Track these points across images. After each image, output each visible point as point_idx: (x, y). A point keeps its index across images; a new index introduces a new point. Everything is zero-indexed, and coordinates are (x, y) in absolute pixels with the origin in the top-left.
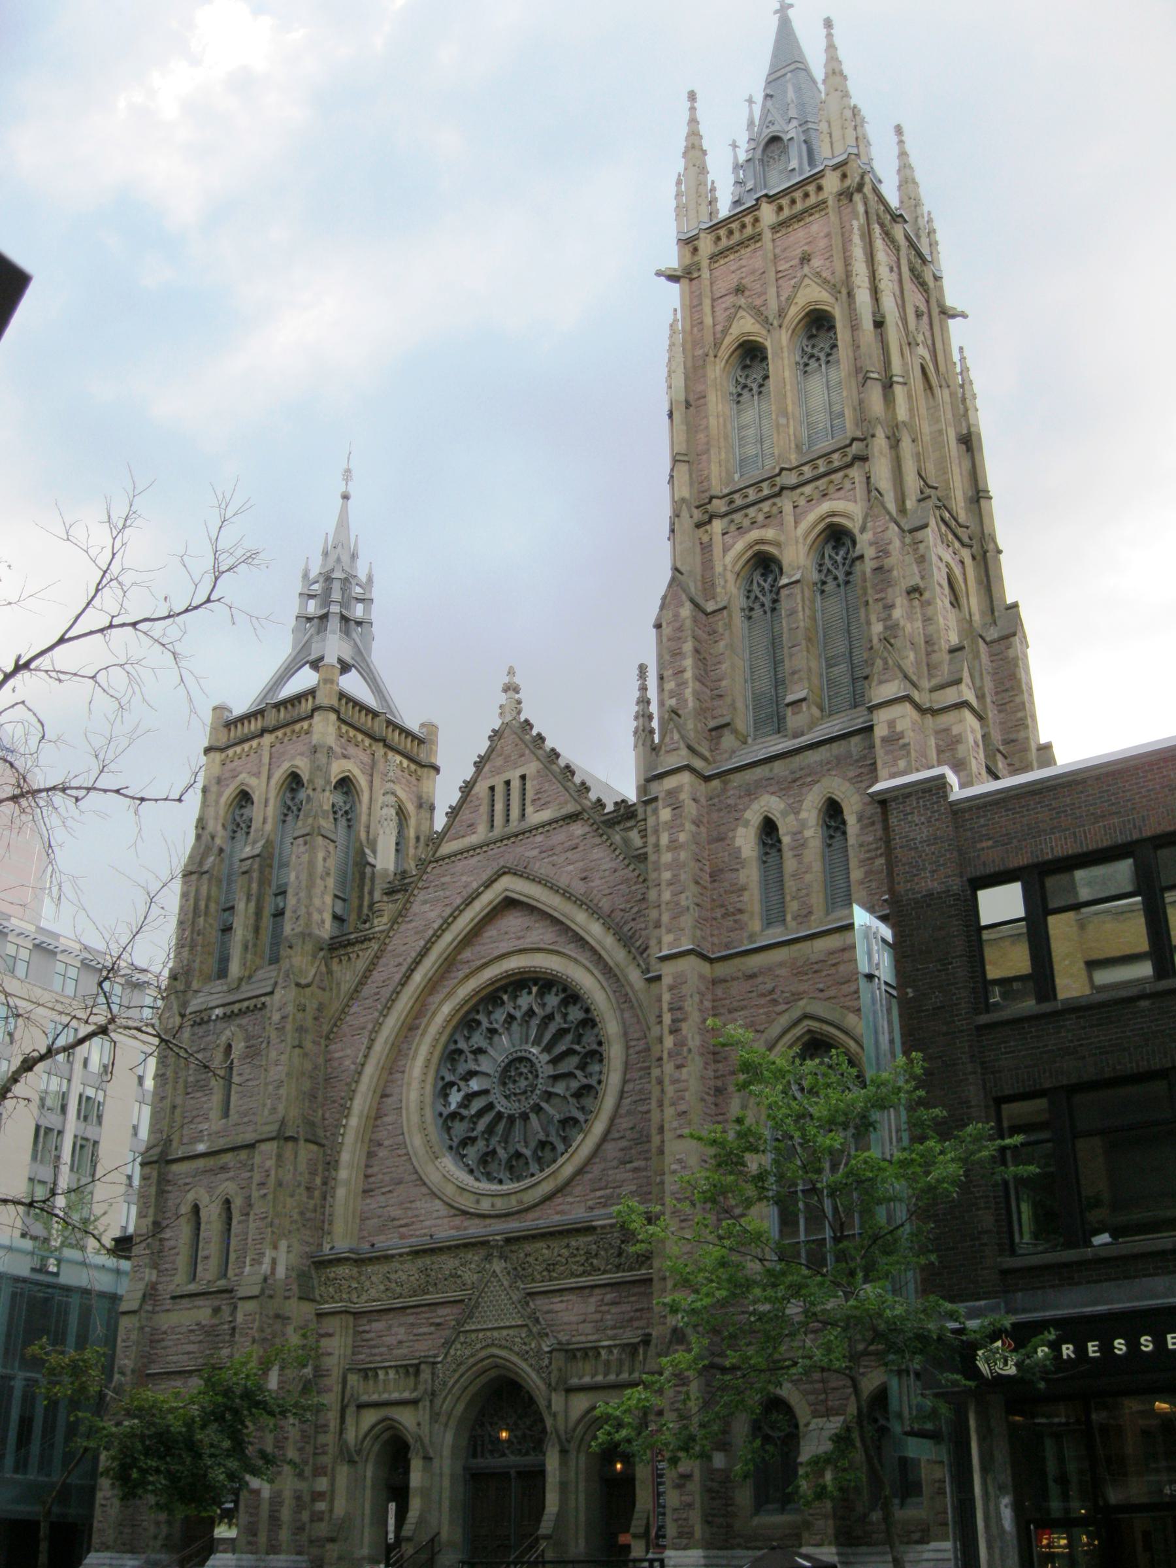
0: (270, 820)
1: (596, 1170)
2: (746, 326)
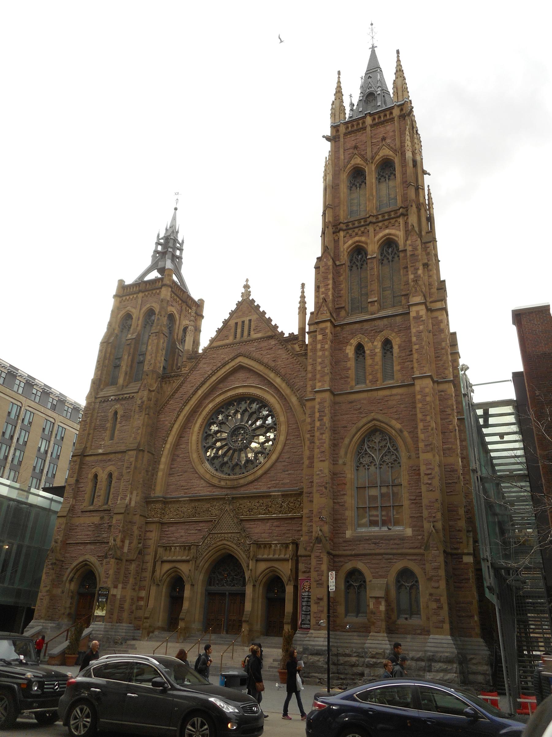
0: (139, 326)
2: (358, 161)
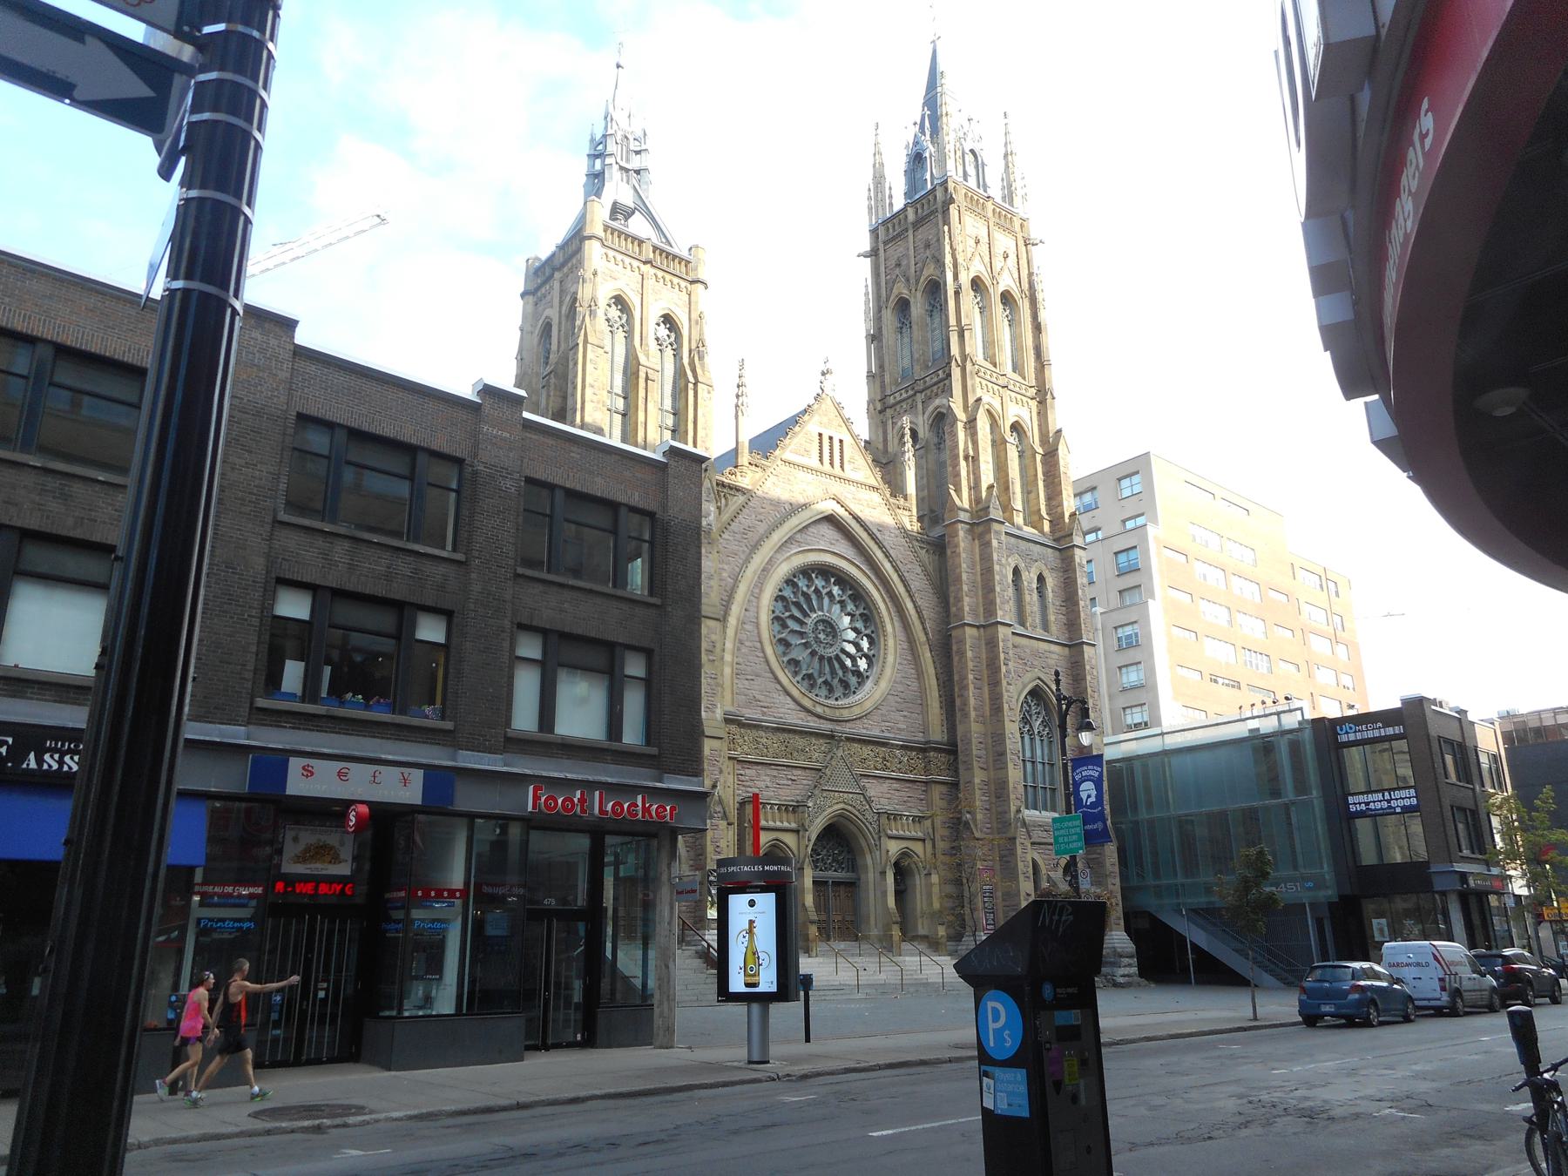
1: (884, 710)
2: (977, 268)
